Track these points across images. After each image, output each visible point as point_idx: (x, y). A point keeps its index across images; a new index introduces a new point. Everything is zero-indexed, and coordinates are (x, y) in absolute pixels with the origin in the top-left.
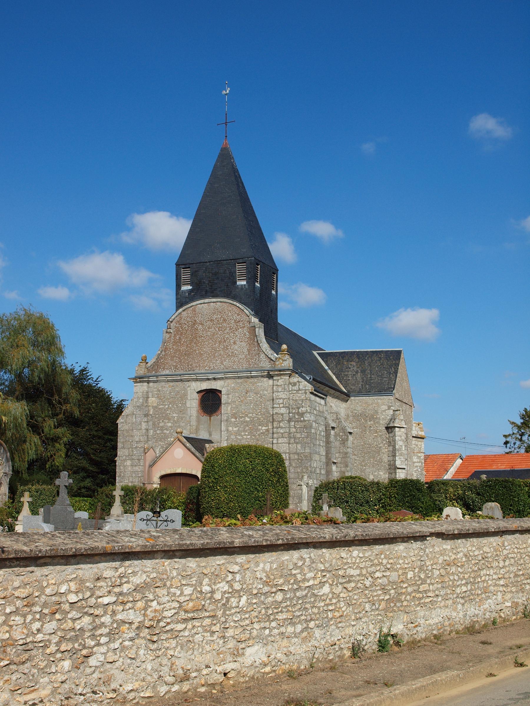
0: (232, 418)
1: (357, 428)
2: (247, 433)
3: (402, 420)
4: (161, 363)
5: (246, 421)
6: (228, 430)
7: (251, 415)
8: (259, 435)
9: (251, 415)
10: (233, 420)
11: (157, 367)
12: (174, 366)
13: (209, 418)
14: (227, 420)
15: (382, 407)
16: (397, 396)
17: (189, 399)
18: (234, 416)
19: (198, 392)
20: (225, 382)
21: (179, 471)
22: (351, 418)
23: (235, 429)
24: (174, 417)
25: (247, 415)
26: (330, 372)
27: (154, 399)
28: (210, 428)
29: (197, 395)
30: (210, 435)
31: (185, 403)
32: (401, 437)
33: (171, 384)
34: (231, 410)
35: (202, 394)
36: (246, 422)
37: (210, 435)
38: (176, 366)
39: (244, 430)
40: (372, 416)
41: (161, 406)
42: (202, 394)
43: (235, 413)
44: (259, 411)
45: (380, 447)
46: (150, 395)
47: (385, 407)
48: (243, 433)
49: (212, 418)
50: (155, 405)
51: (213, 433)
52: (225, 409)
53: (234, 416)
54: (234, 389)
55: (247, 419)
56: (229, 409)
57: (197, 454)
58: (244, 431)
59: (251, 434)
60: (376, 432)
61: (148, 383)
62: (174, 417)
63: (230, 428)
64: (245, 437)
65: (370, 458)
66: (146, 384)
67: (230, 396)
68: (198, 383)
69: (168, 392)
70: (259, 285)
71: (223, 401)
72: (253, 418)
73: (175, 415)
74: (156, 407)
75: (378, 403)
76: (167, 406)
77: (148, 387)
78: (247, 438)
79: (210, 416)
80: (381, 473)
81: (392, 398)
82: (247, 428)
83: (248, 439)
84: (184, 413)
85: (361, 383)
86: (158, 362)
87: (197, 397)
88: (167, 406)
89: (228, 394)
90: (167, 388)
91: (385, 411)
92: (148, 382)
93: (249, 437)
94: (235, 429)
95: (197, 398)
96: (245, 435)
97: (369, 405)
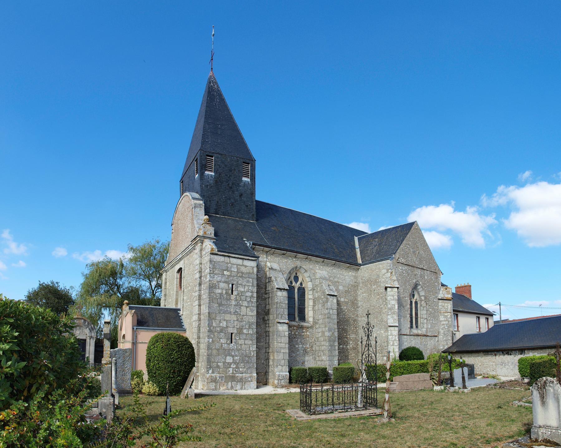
1: (365, 292)
3: (395, 280)
15: (383, 271)
16: (402, 260)
22: (361, 285)
26: (358, 251)
32: (393, 296)
40: (376, 280)
45: (381, 308)
47: (384, 271)
60: (379, 295)
65: (374, 318)
70: (213, 174)
75: (379, 269)
80: (382, 332)
81: (389, 261)
85: (374, 254)
91: (384, 274)
97: (373, 271)
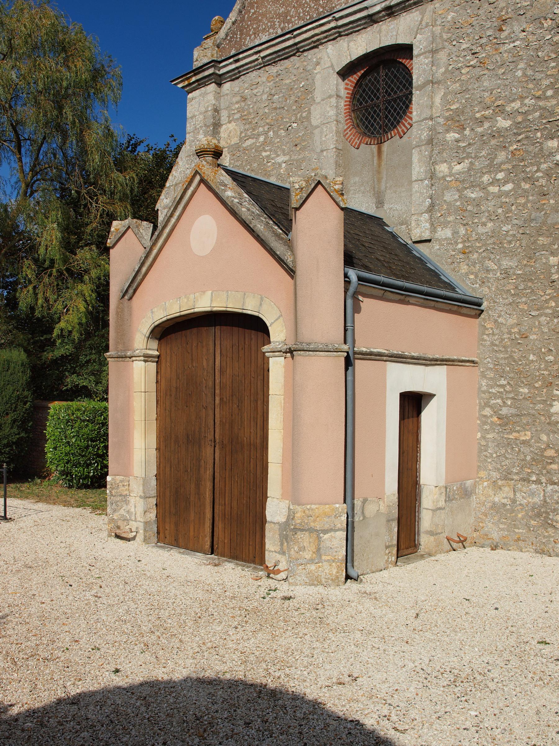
0: (447, 131)
2: (500, 176)
4: (250, 19)
5: (499, 131)
6: (432, 176)
7: (516, 105)
8: (548, 174)
9: (516, 105)
10: (452, 136)
11: (241, 34)
12: (279, 15)
13: (374, 148)
14: (430, 141)
17: (318, 100)
18: (456, 121)
19: (344, 73)
20: (423, 14)
21: (204, 304)
23: (458, 168)
24: (280, 165)
25: (500, 110)
27: (232, 126)
28: (379, 181)
29: (342, 85)
30: (380, 203)
31: (308, 118)
33: (273, 70)
34: (446, 102)
35: (354, 78)
36: (498, 134)
37: (380, 203)
38: (287, 14)
39: (491, 165)
41: (249, 142)
42: (354, 78)
43: (459, 112)
44: (546, 82)
46: (224, 115)
48: (486, 178)
49: (385, 147)
50: (235, 140)
51: (389, 195)
52: (424, 105)
53: (456, 121)
54: (456, 26)
55: (503, 123)
56: (438, 100)
57: (261, 225)
58: (493, 168)
59: (517, 173)
61: (219, 85)
62: (280, 165)
63: (443, 168)
64: (494, 189)
66: (212, 87)
67: (442, 56)
68: (343, 43)
69: (265, 97)
71: (417, 78)
72: (526, 113)
73: (280, 159)
74: (237, 147)
76: (262, 139)
77: (218, 96)
78: (501, 194)
79: (380, 143)
82: (502, 156)
83: (507, 194)
84: (304, 149)
86: (243, 20)
87: (343, 88)
88: (262, 139)
89: (434, 52)
90: (259, 84)
92: (219, 80)
93: (509, 187)
94: (458, 168)
95: (343, 93)
96: (495, 182)
